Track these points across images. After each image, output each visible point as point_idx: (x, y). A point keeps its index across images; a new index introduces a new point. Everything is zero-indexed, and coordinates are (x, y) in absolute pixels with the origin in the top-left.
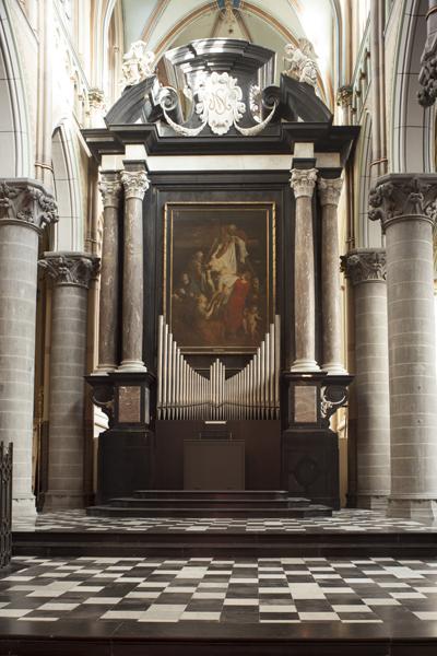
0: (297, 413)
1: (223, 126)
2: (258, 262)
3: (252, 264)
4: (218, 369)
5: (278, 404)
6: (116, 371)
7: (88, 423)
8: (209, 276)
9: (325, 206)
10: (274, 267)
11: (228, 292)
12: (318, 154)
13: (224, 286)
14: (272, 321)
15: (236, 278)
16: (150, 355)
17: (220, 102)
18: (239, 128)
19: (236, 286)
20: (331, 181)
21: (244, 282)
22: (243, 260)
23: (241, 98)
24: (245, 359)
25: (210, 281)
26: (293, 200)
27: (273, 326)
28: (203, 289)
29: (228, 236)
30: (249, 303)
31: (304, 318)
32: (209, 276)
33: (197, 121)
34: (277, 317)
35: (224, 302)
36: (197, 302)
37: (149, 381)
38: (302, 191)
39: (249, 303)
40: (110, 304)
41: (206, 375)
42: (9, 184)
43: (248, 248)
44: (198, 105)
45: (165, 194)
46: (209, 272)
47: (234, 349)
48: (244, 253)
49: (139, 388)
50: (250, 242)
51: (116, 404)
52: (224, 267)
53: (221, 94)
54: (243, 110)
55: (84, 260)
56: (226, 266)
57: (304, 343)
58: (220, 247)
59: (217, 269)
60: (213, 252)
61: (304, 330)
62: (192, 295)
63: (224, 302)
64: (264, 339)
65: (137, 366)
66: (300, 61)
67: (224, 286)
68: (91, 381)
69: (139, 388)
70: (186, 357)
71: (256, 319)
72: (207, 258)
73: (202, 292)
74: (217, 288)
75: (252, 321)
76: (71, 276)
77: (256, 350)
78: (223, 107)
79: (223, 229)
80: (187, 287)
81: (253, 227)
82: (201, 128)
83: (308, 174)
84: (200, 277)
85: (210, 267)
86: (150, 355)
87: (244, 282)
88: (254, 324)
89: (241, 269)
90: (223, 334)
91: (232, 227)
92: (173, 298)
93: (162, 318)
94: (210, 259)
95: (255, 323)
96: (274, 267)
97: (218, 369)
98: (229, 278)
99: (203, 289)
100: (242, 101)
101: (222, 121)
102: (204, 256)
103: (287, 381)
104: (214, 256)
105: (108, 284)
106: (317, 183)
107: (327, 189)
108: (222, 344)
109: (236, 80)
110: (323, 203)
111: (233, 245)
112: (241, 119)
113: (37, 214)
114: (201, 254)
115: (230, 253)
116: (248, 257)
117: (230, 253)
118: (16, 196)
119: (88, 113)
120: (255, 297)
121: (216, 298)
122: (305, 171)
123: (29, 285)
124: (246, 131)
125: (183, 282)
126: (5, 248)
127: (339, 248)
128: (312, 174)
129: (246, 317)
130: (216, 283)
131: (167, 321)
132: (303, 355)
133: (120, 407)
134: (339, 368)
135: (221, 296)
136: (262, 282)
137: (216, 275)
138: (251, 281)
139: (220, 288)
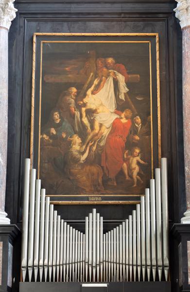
2: (139, 99)
3: (134, 101)
4: (94, 220)
5: (167, 262)
8: (84, 114)
11: (106, 132)
13: (101, 125)
14: (158, 165)
15: (115, 116)
19: (115, 127)
21: (124, 121)
22: (122, 97)
24: (127, 211)
25: (85, 121)
27: (158, 171)
28: (77, 129)
29: (105, 69)
30: (130, 145)
32: (84, 114)
34: (164, 161)
35: (102, 144)
36: (70, 144)
39: (130, 145)
41: (81, 228)
43: (128, 84)
45: (34, 24)
46: (84, 109)
48: (124, 89)
50: (130, 76)
52: (102, 104)
58: (96, 82)
59: (93, 107)
60: (89, 87)
63: (102, 144)
64: (149, 186)
67: (101, 125)
70: (57, 207)
71: (138, 163)
73: (75, 133)
74: (92, 128)
75: (134, 165)
77: (139, 199)
79: (100, 62)
80: (57, 127)
85: (85, 105)
88: (136, 169)
89: (120, 107)
90: (100, 180)
91: (110, 60)
92: (42, 139)
93: (29, 162)
94: (85, 95)
96: (159, 105)
97: (94, 220)
99: (77, 129)
102: (78, 93)
104: (89, 92)
108: (98, 191)
111: (111, 80)
114: (74, 90)
120: (137, 138)
121: (91, 140)
125: (53, 120)
129: (127, 160)
130: (92, 122)
131: (35, 165)
135: (97, 138)
136: (145, 122)
137: (91, 113)
138: (132, 119)
139: (97, 127)
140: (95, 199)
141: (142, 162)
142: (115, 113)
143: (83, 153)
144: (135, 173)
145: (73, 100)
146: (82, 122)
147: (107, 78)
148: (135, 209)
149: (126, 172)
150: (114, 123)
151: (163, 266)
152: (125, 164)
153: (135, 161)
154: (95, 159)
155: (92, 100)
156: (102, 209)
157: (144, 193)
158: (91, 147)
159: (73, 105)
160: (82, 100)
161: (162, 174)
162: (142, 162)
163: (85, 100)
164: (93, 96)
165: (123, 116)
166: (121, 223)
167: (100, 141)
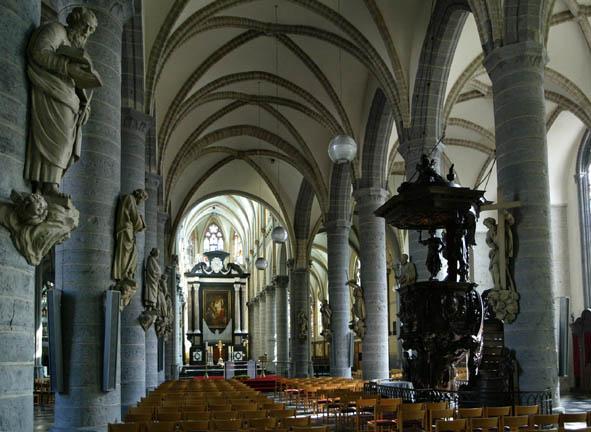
3: (225, 305)
4: (217, 331)
16: (201, 329)
17: (217, 265)
33: (210, 269)
37: (201, 335)
38: (237, 288)
56: (218, 306)
65: (199, 332)
81: (225, 297)
86: (201, 329)
97: (217, 331)
98: (219, 309)
103: (234, 335)
127: (246, 300)
134: (246, 331)
154: (217, 318)
155: (216, 305)
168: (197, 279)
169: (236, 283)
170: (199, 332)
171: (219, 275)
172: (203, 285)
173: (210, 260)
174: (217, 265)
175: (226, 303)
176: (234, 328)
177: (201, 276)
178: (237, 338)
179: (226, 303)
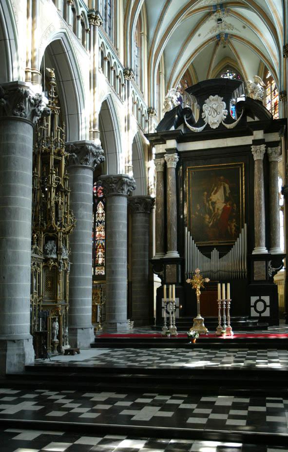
0: (255, 276)
1: (216, 123)
3: (232, 197)
4: (215, 253)
5: (246, 270)
6: (164, 257)
7: (151, 282)
9: (271, 162)
10: (244, 197)
11: (220, 212)
12: (266, 134)
13: (218, 209)
14: (243, 227)
15: (224, 204)
18: (224, 124)
19: (225, 209)
20: (274, 148)
21: (228, 206)
22: (227, 195)
23: (225, 108)
24: (229, 248)
25: (211, 207)
26: (254, 162)
27: (243, 230)
28: (207, 211)
31: (259, 225)
33: (201, 122)
34: (245, 225)
35: (219, 218)
36: (204, 219)
37: (181, 261)
38: (258, 154)
40: (160, 221)
41: (209, 256)
42: (114, 177)
43: (230, 188)
44: (203, 114)
46: (210, 202)
47: (222, 242)
48: (228, 191)
49: (176, 265)
51: (165, 273)
52: (218, 199)
53: (215, 106)
54: (227, 114)
55: (147, 199)
56: (218, 198)
57: (260, 238)
58: (215, 189)
59: (214, 201)
61: (260, 232)
62: (202, 215)
64: (239, 237)
65: (175, 254)
66: (255, 88)
67: (218, 209)
68: (152, 261)
69: (176, 265)
70: (199, 248)
71: (235, 226)
72: (209, 195)
74: (214, 211)
76: (141, 208)
78: (216, 113)
81: (232, 177)
82: (205, 126)
83: (260, 148)
84: (206, 205)
85: (211, 200)
86: (181, 249)
87: (228, 206)
88: (234, 228)
89: (227, 200)
91: (222, 178)
93: (186, 228)
94: (211, 195)
95: (234, 228)
96: (244, 197)
97: (215, 253)
100: (226, 109)
101: (216, 121)
103: (252, 259)
104: (213, 193)
105: (159, 212)
106: (266, 150)
107: (272, 153)
108: (217, 240)
109: (222, 98)
110: (270, 160)
111: (222, 187)
112: (225, 119)
113: (126, 188)
114: (206, 193)
115: (221, 192)
116: (230, 193)
117: (221, 192)
118: (117, 183)
119: (147, 121)
122: (258, 146)
123: (124, 224)
124: (228, 126)
126: (113, 207)
128: (263, 147)
129: (229, 225)
130: (214, 208)
132: (259, 245)
133: (167, 275)
137: (214, 203)
138: (232, 205)
139: (216, 210)
140: (215, 243)
141: (236, 225)
142: (224, 203)
143: (210, 223)
144: (233, 230)
145: (205, 198)
146: (209, 208)
147: (220, 186)
148: (233, 247)
149: (229, 230)
150: (224, 208)
151: (245, 272)
152: (229, 227)
153: (233, 225)
156: (218, 248)
157: (236, 239)
158: (213, 220)
159: (205, 201)
160: (209, 197)
161: (244, 231)
162: (236, 225)
163: (211, 198)
164: (215, 196)
165: (228, 204)
166: (226, 253)
167: (217, 216)
168: (172, 144)
169: (256, 142)
170: (175, 254)
171: (221, 133)
172: (185, 158)
173: (201, 103)
174: (215, 111)
175: (235, 191)
176: (251, 243)
177: (181, 139)
178: (259, 266)
179: (235, 191)
